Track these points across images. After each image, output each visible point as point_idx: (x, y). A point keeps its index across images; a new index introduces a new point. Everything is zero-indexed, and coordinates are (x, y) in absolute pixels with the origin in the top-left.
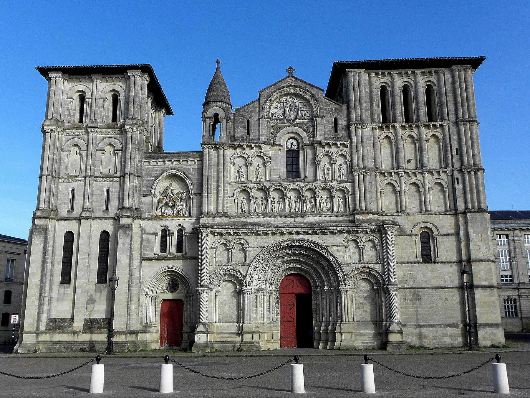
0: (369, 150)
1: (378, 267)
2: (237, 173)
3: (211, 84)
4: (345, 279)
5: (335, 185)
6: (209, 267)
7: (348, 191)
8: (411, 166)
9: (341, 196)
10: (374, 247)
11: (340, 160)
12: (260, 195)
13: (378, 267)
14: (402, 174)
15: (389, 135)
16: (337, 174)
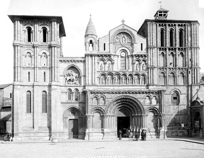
0: (155, 59)
1: (158, 107)
2: (100, 67)
3: (87, 28)
4: (144, 111)
5: (140, 73)
6: (90, 106)
7: (146, 76)
8: (172, 66)
9: (143, 78)
10: (156, 99)
11: (143, 63)
12: (109, 77)
13: (158, 107)
14: (168, 69)
15: (164, 52)
16: (142, 68)
